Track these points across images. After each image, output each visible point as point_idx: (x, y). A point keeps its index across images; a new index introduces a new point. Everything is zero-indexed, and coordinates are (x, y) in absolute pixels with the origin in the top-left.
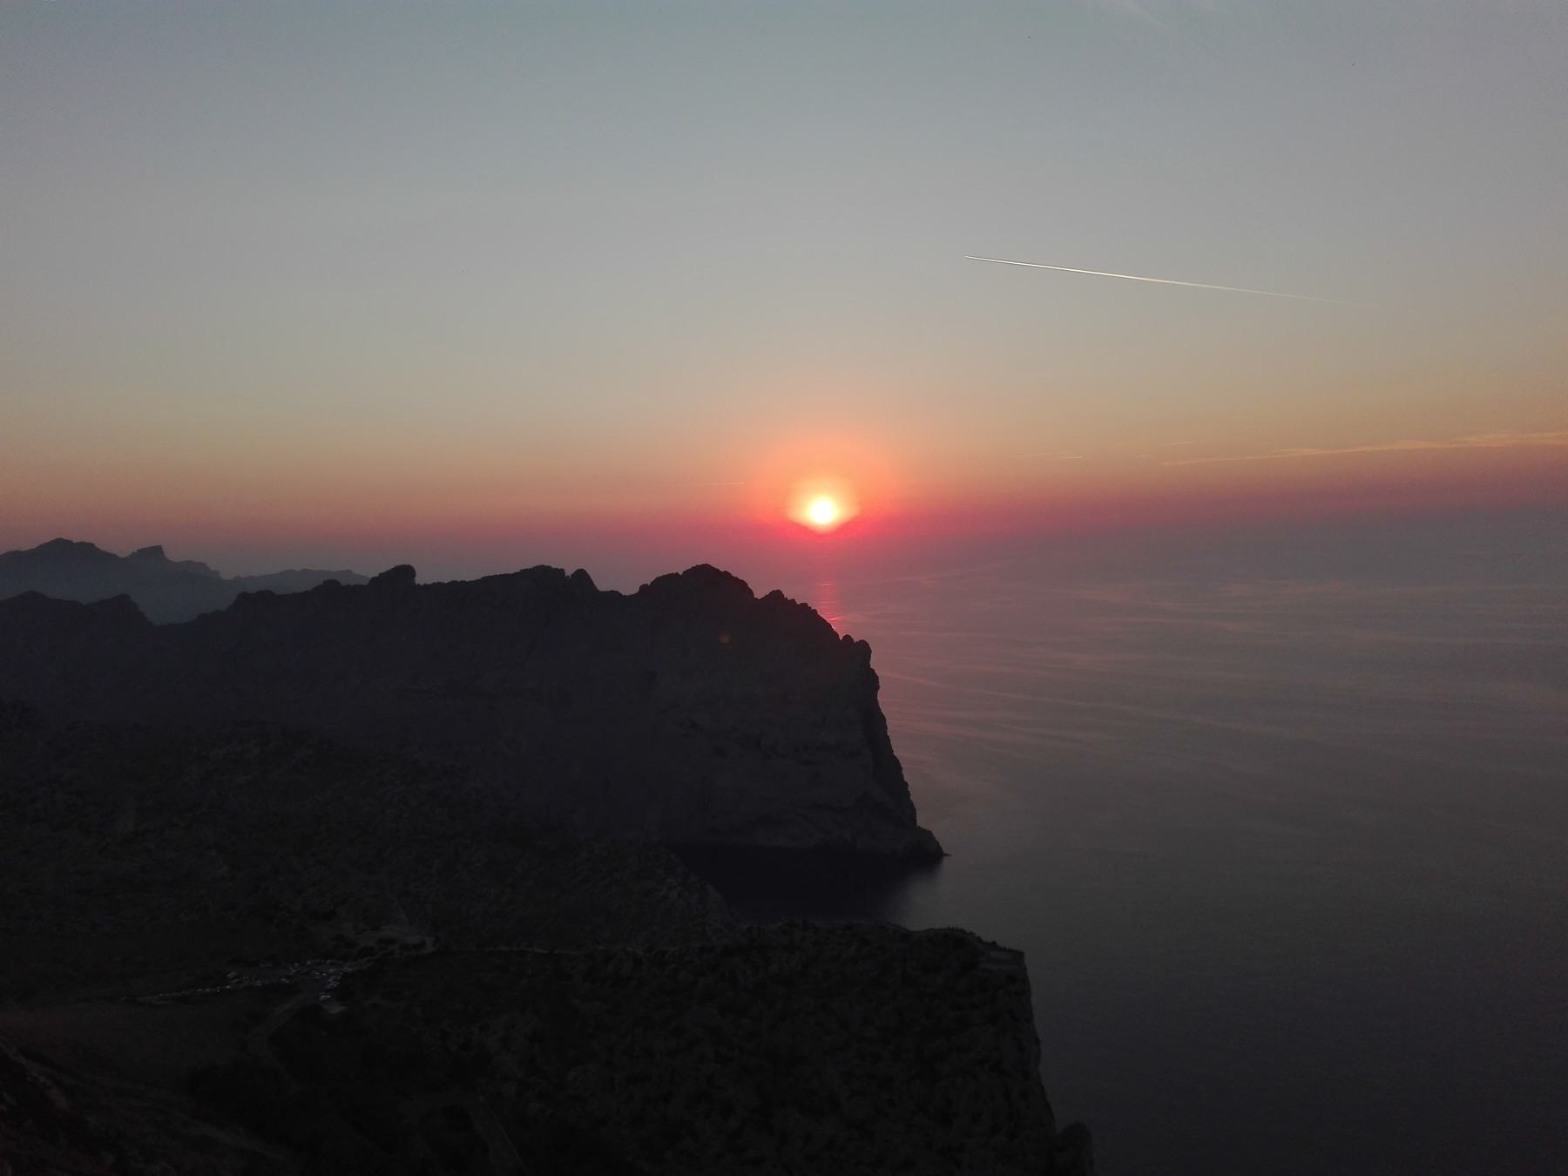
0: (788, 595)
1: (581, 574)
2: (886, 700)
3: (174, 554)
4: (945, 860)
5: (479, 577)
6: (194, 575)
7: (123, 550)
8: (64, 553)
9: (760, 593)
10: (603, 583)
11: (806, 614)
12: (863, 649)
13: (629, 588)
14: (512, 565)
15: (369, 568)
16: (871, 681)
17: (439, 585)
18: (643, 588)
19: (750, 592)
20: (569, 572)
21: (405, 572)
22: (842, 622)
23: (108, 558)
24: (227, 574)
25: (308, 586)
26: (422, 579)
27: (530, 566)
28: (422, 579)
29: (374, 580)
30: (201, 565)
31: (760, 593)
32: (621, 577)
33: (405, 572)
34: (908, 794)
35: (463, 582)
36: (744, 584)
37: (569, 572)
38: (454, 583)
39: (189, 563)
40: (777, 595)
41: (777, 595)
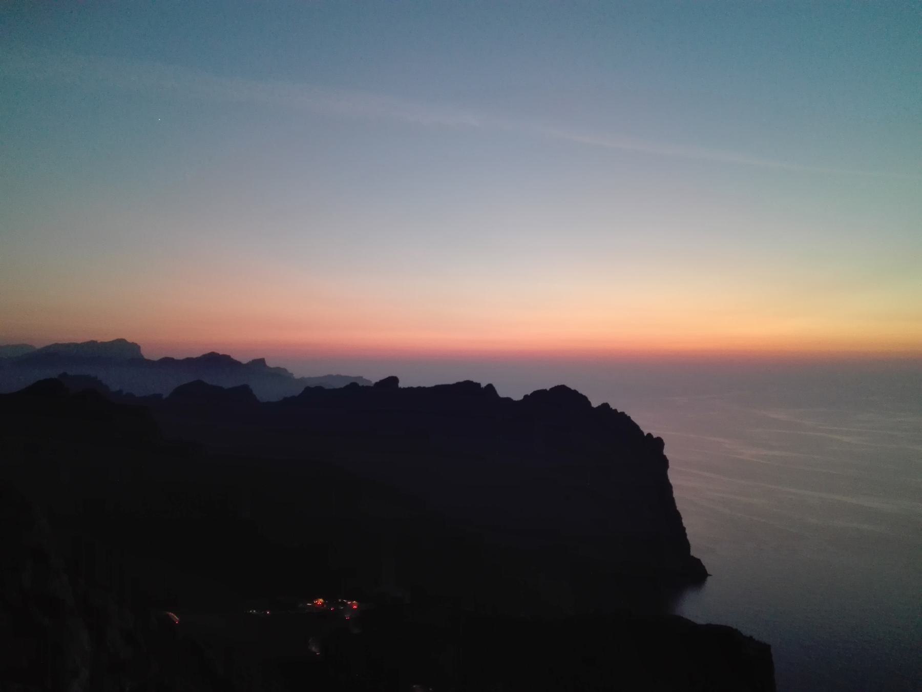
0: (613, 406)
1: (490, 387)
2: (673, 476)
3: (270, 363)
4: (709, 578)
5: (433, 385)
6: (279, 374)
7: (244, 362)
8: (216, 361)
9: (595, 403)
10: (502, 393)
11: (624, 421)
12: (658, 443)
13: (518, 397)
14: (451, 379)
15: (374, 377)
16: (664, 463)
17: (410, 390)
18: (526, 396)
19: (589, 403)
20: (483, 385)
21: (393, 380)
22: (648, 424)
23: (237, 363)
24: (297, 375)
25: (342, 385)
26: (401, 385)
27: (461, 380)
28: (401, 385)
29: (376, 384)
30: (285, 370)
31: (595, 403)
32: (513, 389)
33: (393, 380)
34: (686, 535)
35: (424, 388)
36: (585, 398)
37: (483, 385)
38: (419, 388)
39: (279, 368)
40: (605, 406)
41: (605, 406)
